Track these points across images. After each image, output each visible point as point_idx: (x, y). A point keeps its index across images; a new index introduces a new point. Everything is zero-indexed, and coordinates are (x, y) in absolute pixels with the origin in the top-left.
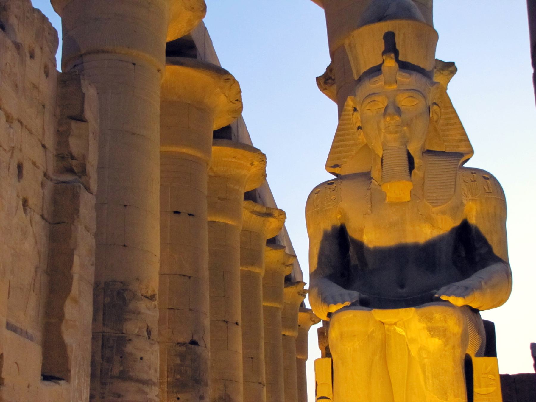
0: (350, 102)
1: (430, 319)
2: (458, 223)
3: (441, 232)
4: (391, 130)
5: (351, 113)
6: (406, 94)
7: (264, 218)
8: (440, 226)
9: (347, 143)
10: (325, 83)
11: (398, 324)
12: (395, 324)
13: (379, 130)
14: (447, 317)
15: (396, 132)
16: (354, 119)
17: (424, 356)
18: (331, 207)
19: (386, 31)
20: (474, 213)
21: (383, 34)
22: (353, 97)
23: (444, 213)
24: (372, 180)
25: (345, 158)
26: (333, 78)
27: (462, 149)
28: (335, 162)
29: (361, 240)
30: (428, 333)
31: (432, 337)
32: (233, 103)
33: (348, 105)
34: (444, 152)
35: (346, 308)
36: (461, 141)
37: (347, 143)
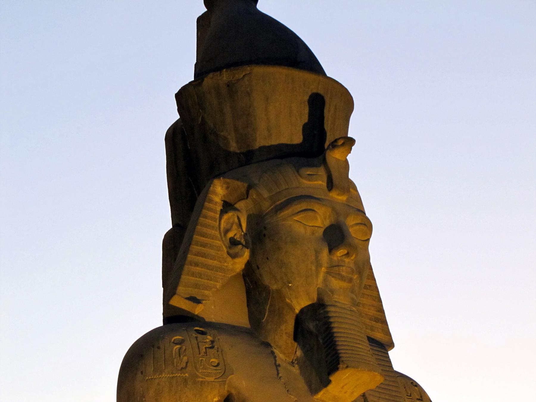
4: (344, 274)
5: (219, 208)
9: (210, 262)
13: (319, 265)
15: (350, 280)
18: (212, 379)
19: (315, 91)
21: (310, 94)
33: (215, 194)
37: (210, 262)
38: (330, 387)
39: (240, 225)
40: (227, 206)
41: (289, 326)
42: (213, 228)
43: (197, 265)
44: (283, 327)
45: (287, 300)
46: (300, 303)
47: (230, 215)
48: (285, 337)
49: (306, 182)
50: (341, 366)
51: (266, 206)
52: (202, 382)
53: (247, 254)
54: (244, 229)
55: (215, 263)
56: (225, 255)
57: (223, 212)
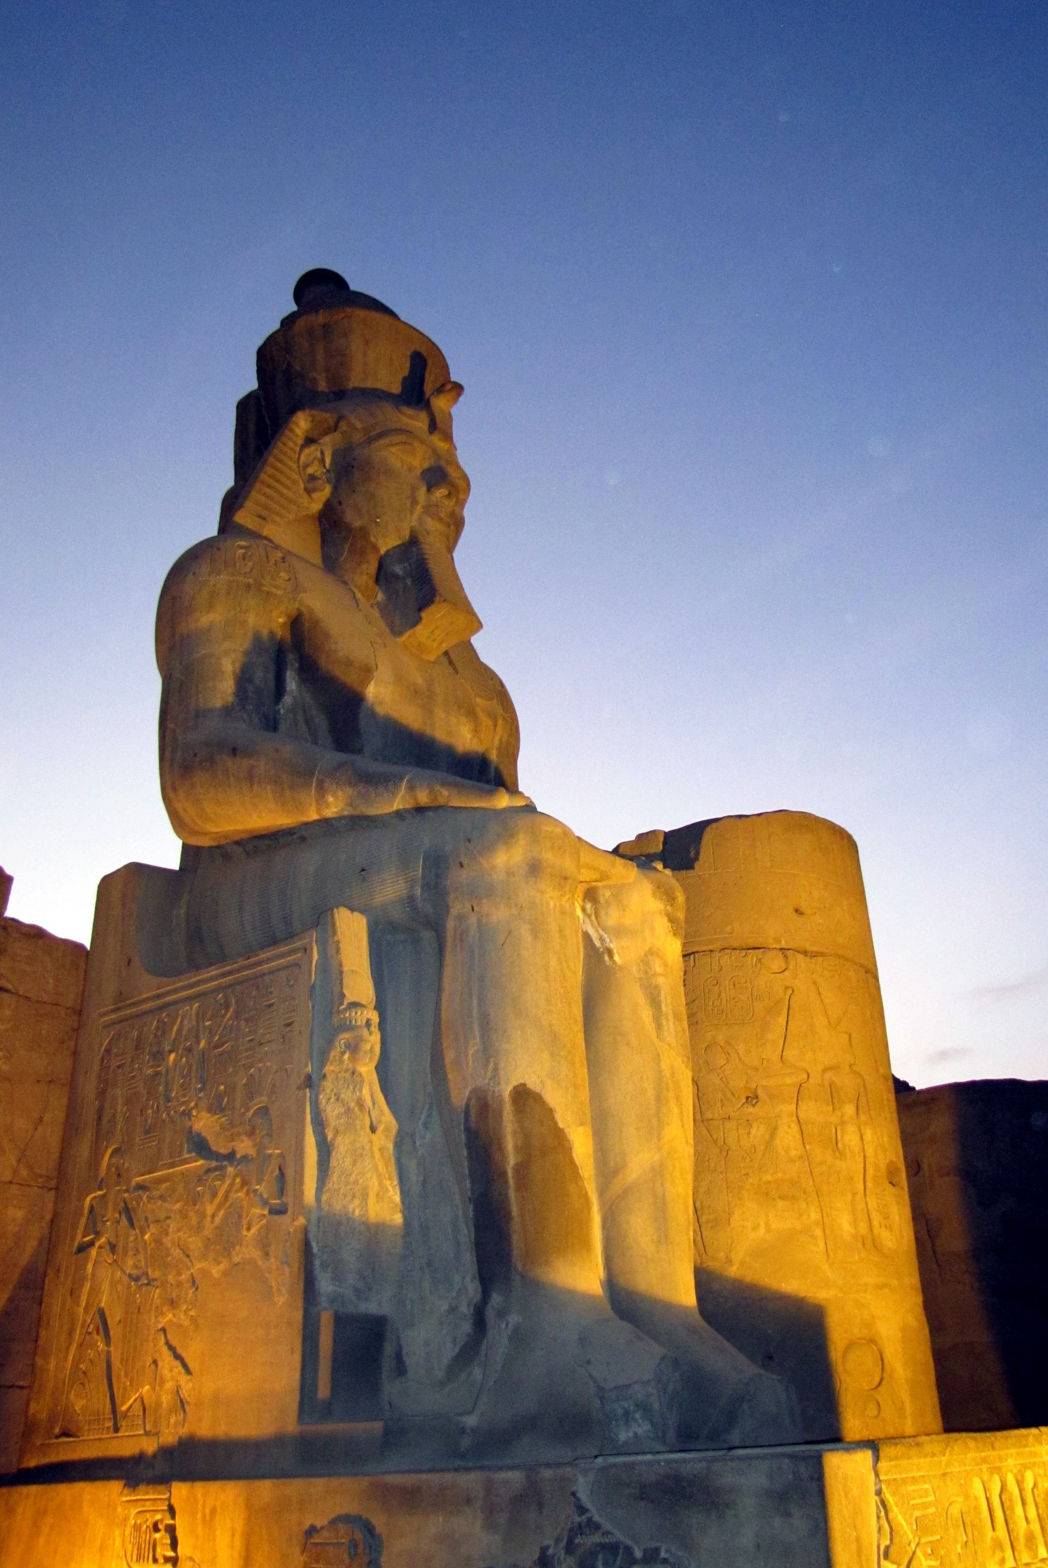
5: (300, 442)
9: (285, 491)
16: (302, 458)
17: (659, 970)
19: (418, 349)
22: (329, 418)
25: (277, 514)
37: (285, 491)
38: (419, 628)
39: (323, 461)
40: (309, 441)
41: (373, 567)
42: (291, 459)
43: (269, 486)
44: (364, 567)
45: (372, 539)
46: (387, 542)
47: (312, 451)
48: (365, 577)
49: (406, 420)
50: (437, 599)
51: (358, 437)
52: (268, 593)
53: (327, 490)
54: (327, 465)
55: (290, 494)
56: (302, 491)
57: (302, 447)
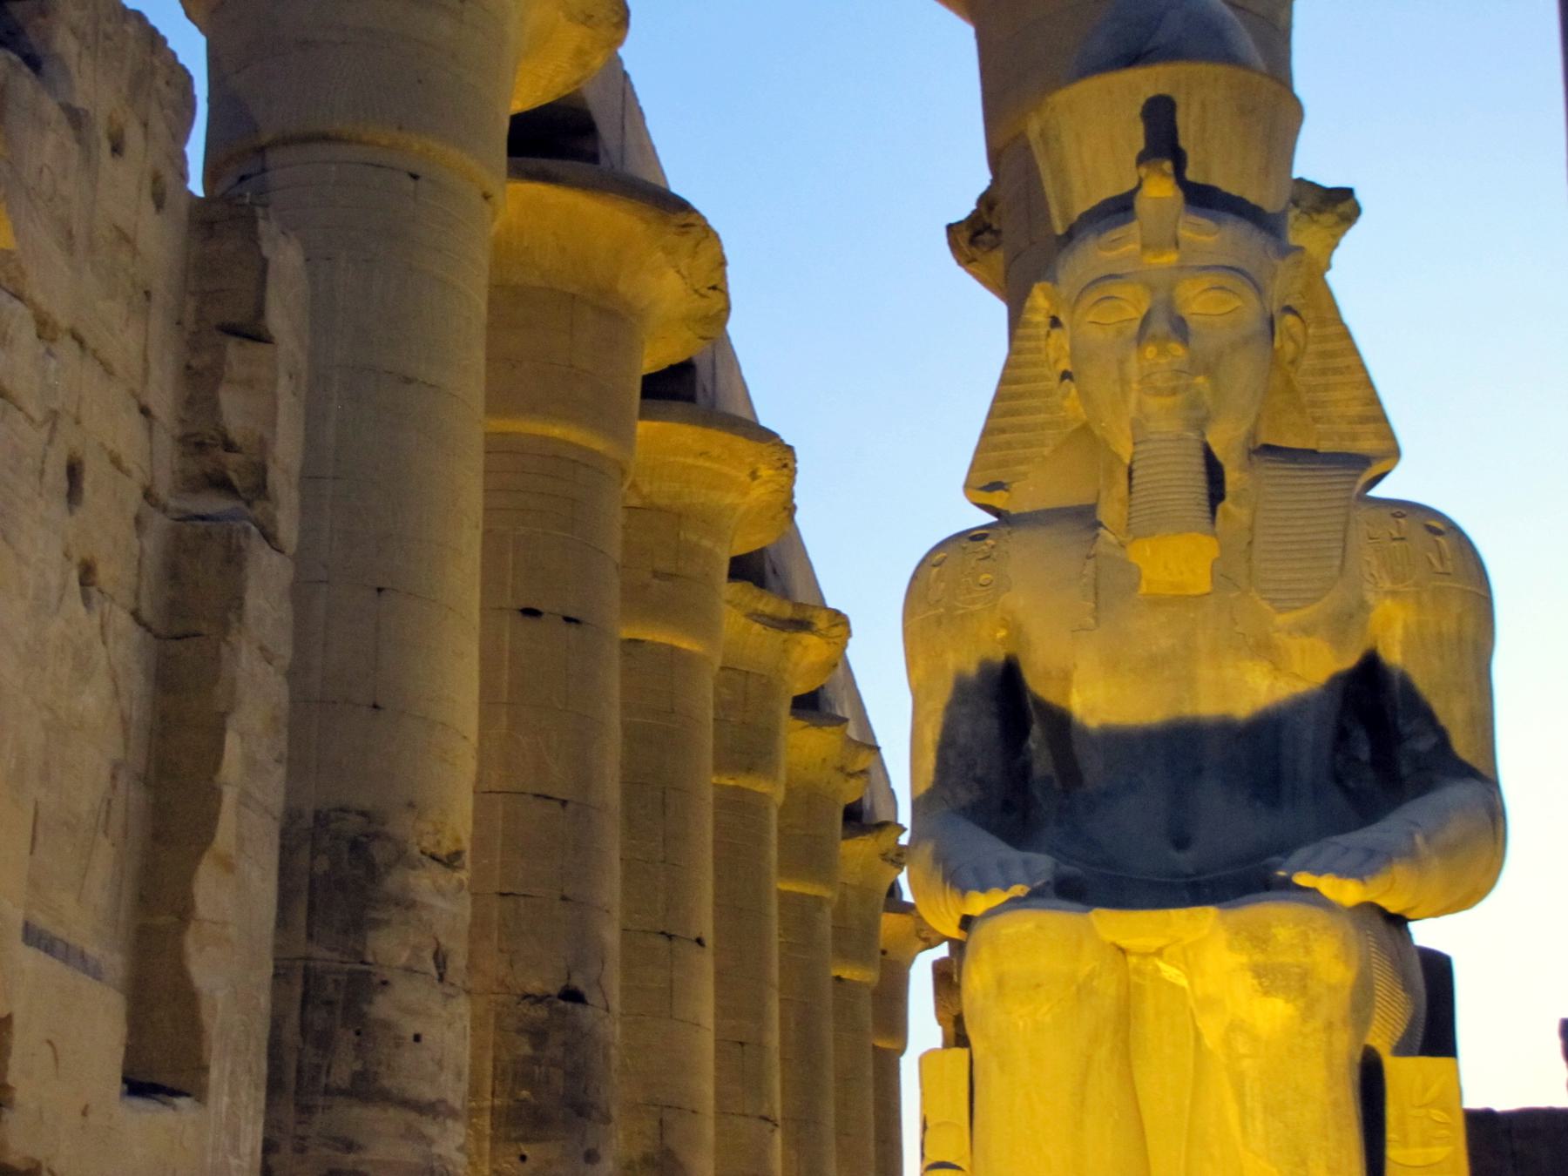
0: (1040, 300)
1: (1260, 940)
2: (1350, 660)
3: (1301, 687)
4: (1159, 384)
5: (1043, 331)
6: (1206, 281)
7: (785, 635)
8: (1298, 670)
9: (1028, 419)
10: (973, 241)
11: (1166, 952)
12: (1159, 953)
13: (1124, 381)
14: (1312, 936)
15: (1174, 392)
17: (1243, 1050)
19: (1151, 94)
20: (1398, 630)
21: (1142, 101)
22: (1048, 285)
23: (1307, 630)
24: (1102, 531)
25: (1021, 462)
26: (995, 226)
27: (1366, 446)
28: (995, 475)
29: (1063, 705)
30: (1255, 982)
31: (1266, 993)
32: (703, 296)
33: (1035, 310)
34: (1314, 452)
35: (1015, 903)
36: (1364, 420)
52: (962, 616)
